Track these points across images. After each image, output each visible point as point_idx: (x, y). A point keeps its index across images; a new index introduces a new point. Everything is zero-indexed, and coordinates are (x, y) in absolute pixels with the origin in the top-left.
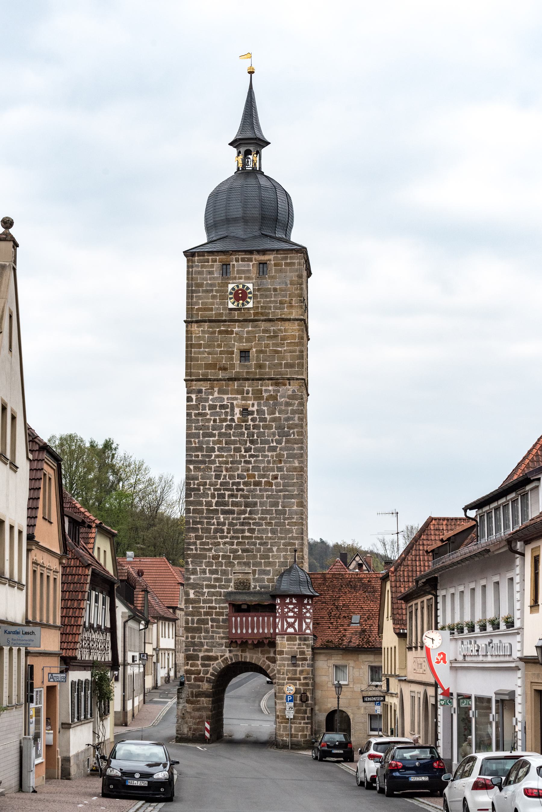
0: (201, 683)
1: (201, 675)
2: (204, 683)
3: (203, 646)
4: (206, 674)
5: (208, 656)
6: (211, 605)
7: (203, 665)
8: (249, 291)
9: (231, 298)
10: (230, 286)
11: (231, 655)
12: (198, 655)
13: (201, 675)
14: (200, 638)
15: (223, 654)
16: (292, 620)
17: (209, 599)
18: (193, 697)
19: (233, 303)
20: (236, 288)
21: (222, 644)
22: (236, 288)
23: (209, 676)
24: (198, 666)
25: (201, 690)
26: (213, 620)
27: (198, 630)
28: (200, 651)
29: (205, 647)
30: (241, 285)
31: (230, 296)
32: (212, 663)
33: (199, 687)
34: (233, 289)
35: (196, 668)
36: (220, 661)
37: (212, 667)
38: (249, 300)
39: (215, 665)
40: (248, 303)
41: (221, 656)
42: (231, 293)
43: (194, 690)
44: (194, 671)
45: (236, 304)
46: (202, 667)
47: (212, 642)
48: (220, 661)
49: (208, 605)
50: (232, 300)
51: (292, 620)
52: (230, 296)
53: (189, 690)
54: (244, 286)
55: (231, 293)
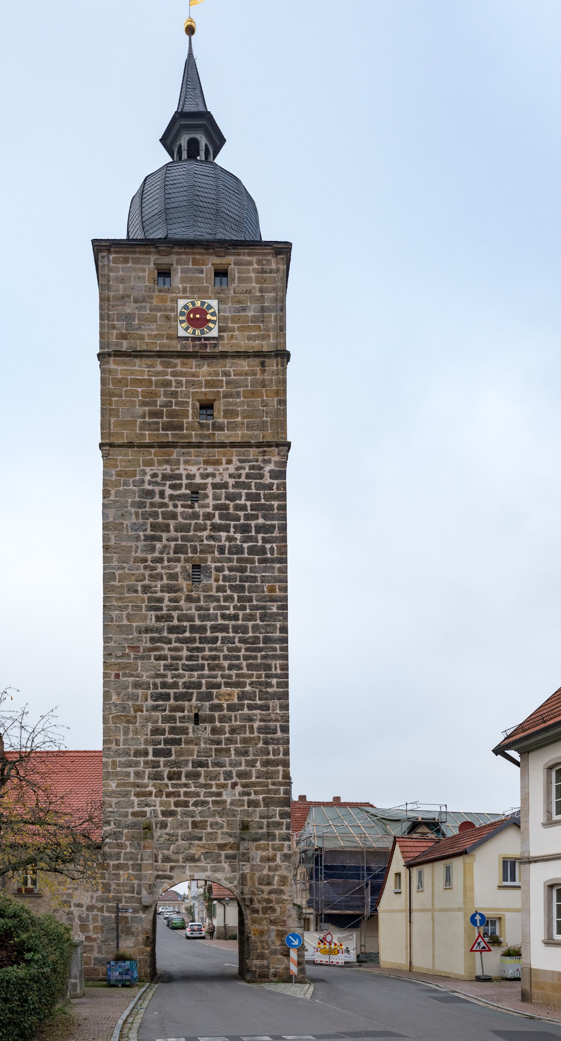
8: (212, 311)
9: (182, 322)
10: (181, 303)
19: (186, 329)
20: (191, 306)
22: (191, 306)
30: (199, 302)
31: (181, 318)
34: (186, 307)
38: (211, 325)
40: (210, 329)
42: (182, 314)
45: (191, 330)
50: (185, 325)
52: (181, 318)
54: (203, 304)
55: (182, 314)
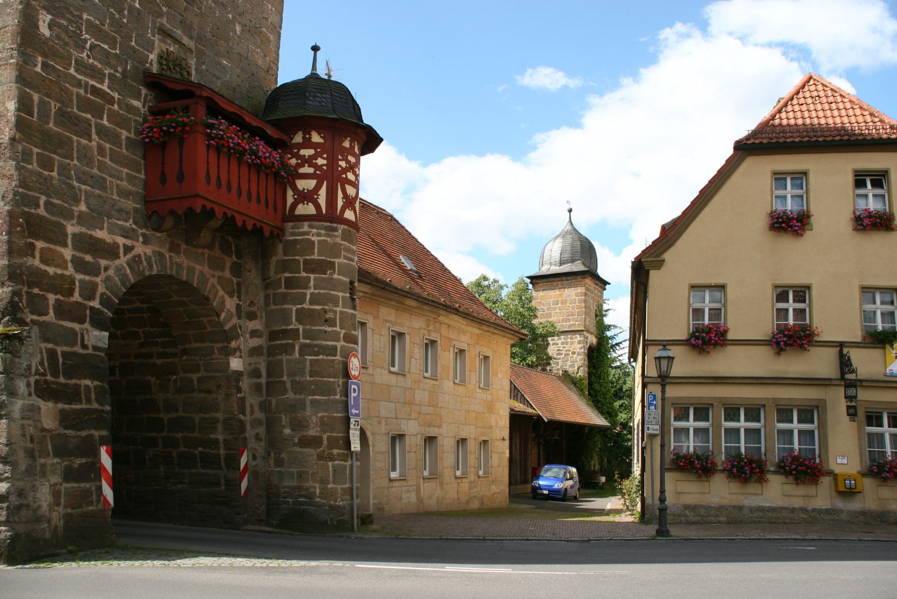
0: (76, 326)
1: (77, 297)
2: (87, 325)
3: (77, 201)
4: (91, 298)
5: (91, 237)
6: (98, 86)
7: (80, 265)
11: (149, 250)
12: (64, 227)
13: (77, 297)
14: (64, 170)
15: (129, 242)
16: (311, 184)
17: (92, 65)
18: (55, 374)
21: (128, 213)
23: (95, 304)
24: (63, 265)
25: (78, 349)
26: (102, 132)
27: (61, 145)
28: (69, 215)
29: (83, 207)
32: (103, 263)
33: (71, 337)
35: (59, 271)
36: (123, 260)
37: (103, 275)
39: (111, 272)
41: (128, 249)
43: (59, 350)
44: (52, 277)
46: (77, 270)
47: (99, 196)
48: (123, 260)
49: (92, 82)
51: (311, 184)
53: (43, 345)
